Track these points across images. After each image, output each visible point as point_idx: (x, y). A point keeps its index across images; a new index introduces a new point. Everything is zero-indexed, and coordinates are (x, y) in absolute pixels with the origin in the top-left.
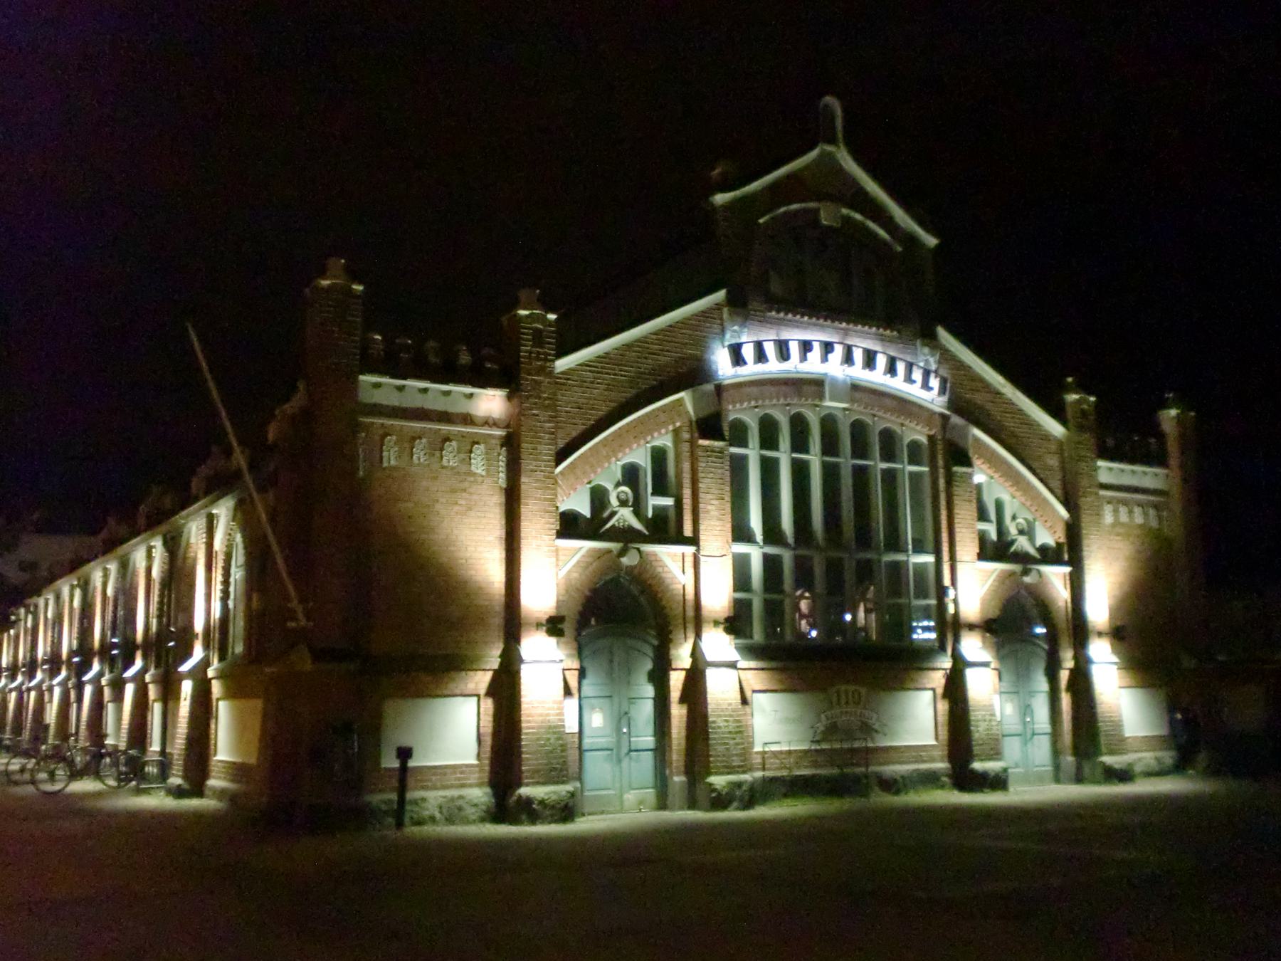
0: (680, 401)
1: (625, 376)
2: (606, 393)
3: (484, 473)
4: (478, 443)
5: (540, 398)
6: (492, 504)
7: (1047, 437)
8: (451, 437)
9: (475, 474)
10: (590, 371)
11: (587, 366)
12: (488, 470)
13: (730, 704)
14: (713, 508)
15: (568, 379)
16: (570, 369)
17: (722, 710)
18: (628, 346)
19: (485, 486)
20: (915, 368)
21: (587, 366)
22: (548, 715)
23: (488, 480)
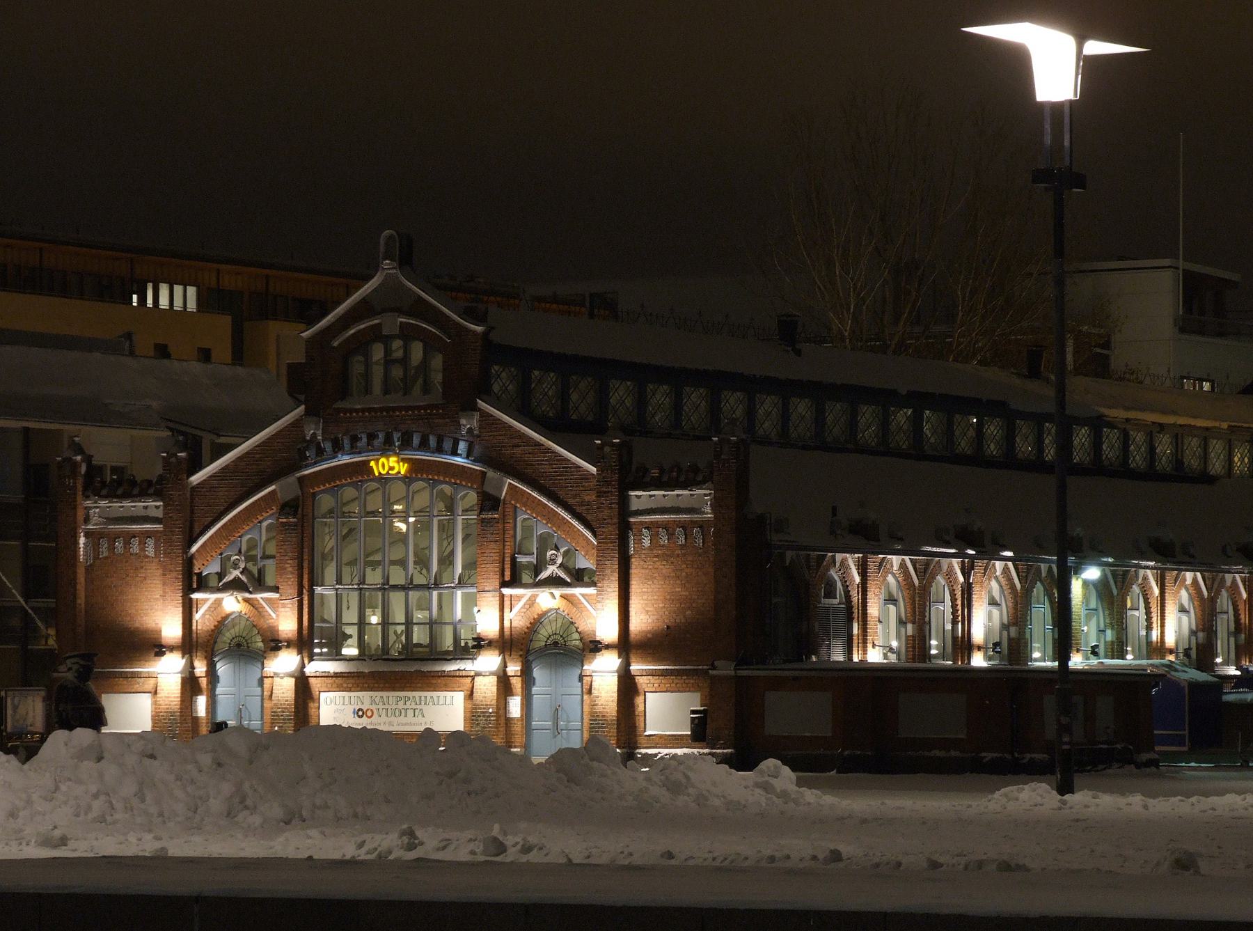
0: (273, 492)
1: (238, 479)
2: (226, 493)
3: (153, 556)
4: (150, 537)
5: (173, 505)
6: (158, 575)
7: (586, 475)
8: (136, 535)
9: (147, 557)
10: (216, 480)
11: (215, 476)
12: (155, 554)
13: (287, 701)
14: (289, 565)
15: (203, 488)
16: (204, 480)
17: (281, 704)
18: (240, 459)
19: (154, 564)
20: (446, 439)
21: (215, 476)
22: (170, 705)
23: (156, 560)
